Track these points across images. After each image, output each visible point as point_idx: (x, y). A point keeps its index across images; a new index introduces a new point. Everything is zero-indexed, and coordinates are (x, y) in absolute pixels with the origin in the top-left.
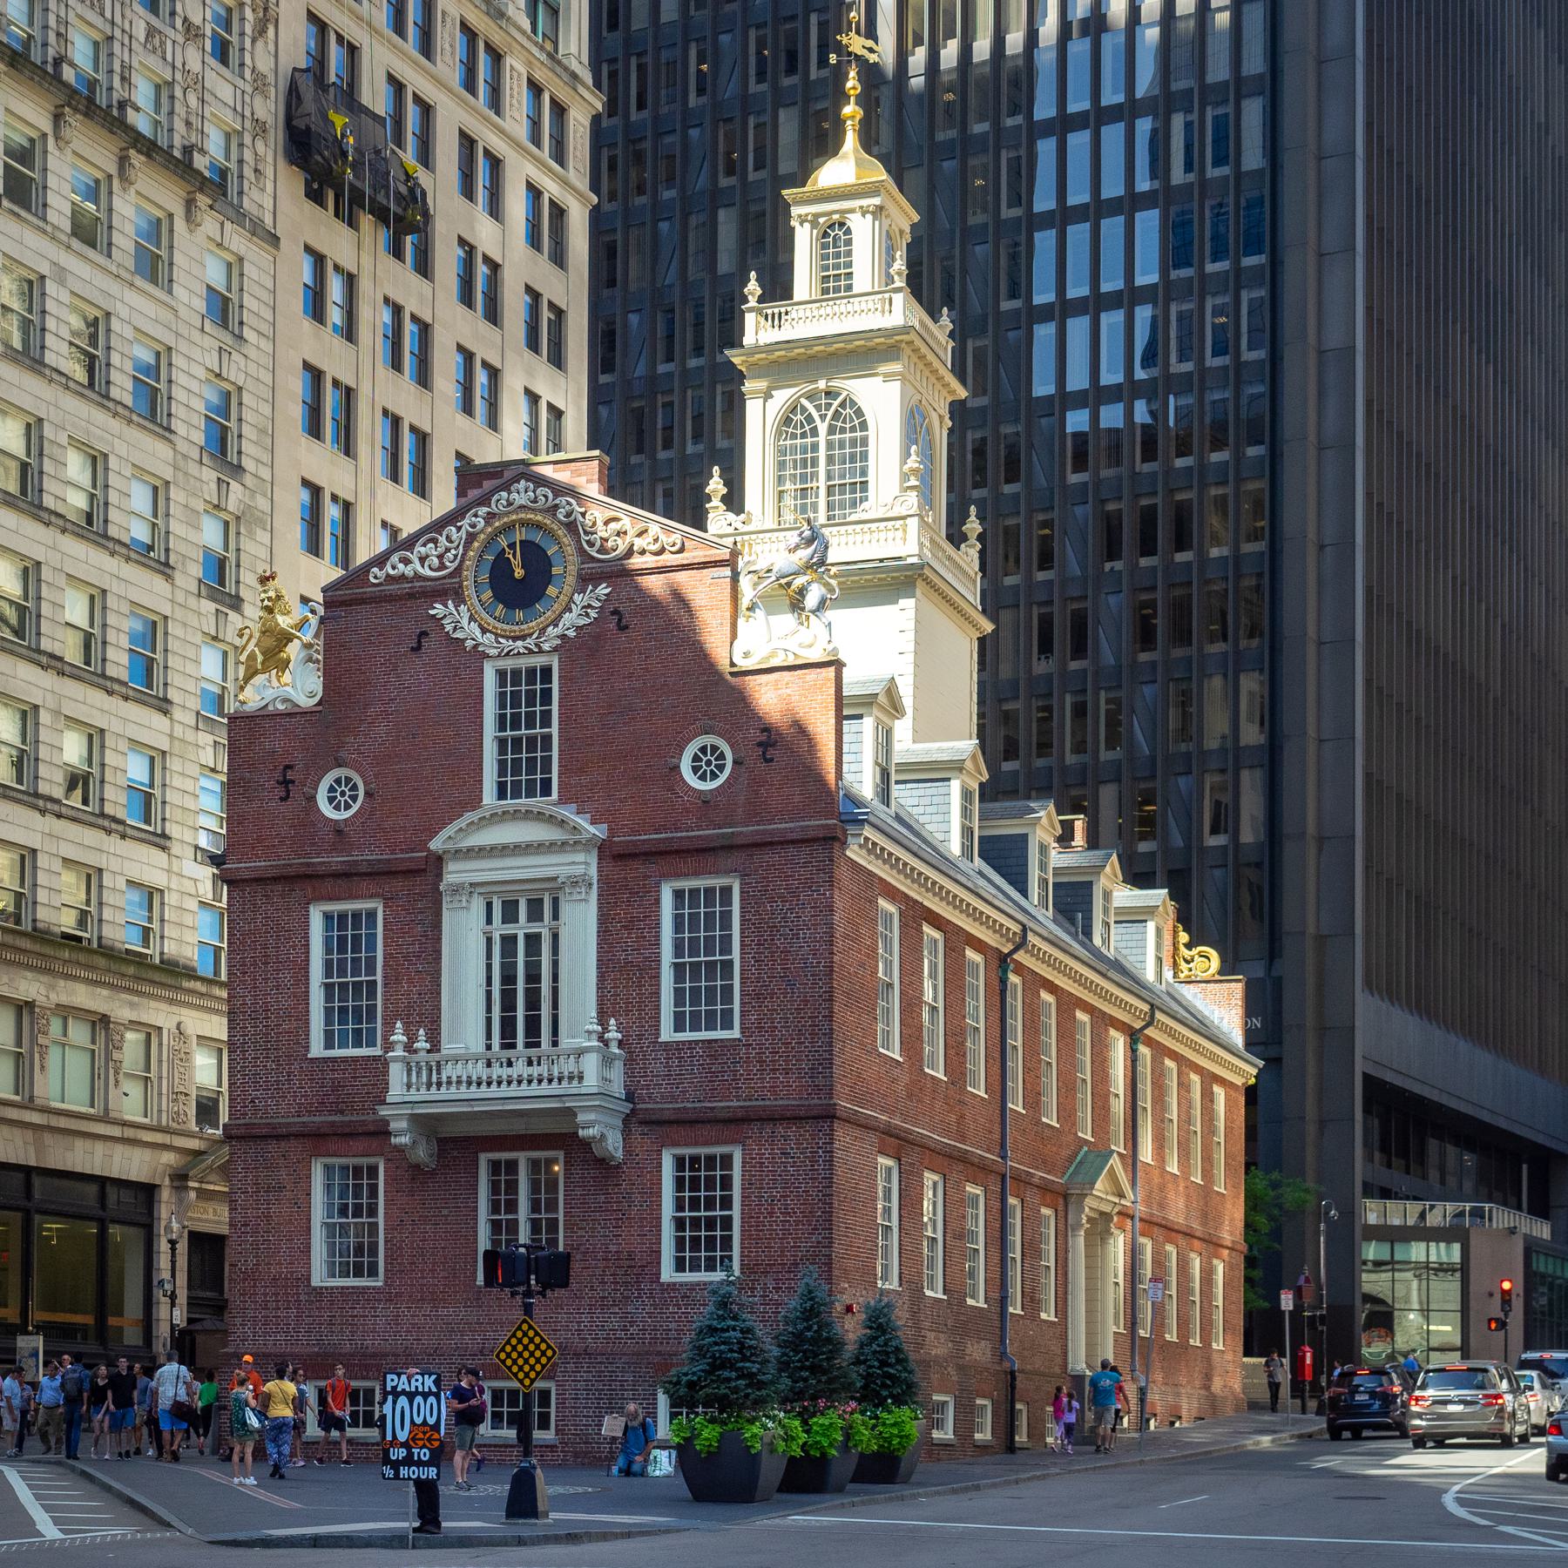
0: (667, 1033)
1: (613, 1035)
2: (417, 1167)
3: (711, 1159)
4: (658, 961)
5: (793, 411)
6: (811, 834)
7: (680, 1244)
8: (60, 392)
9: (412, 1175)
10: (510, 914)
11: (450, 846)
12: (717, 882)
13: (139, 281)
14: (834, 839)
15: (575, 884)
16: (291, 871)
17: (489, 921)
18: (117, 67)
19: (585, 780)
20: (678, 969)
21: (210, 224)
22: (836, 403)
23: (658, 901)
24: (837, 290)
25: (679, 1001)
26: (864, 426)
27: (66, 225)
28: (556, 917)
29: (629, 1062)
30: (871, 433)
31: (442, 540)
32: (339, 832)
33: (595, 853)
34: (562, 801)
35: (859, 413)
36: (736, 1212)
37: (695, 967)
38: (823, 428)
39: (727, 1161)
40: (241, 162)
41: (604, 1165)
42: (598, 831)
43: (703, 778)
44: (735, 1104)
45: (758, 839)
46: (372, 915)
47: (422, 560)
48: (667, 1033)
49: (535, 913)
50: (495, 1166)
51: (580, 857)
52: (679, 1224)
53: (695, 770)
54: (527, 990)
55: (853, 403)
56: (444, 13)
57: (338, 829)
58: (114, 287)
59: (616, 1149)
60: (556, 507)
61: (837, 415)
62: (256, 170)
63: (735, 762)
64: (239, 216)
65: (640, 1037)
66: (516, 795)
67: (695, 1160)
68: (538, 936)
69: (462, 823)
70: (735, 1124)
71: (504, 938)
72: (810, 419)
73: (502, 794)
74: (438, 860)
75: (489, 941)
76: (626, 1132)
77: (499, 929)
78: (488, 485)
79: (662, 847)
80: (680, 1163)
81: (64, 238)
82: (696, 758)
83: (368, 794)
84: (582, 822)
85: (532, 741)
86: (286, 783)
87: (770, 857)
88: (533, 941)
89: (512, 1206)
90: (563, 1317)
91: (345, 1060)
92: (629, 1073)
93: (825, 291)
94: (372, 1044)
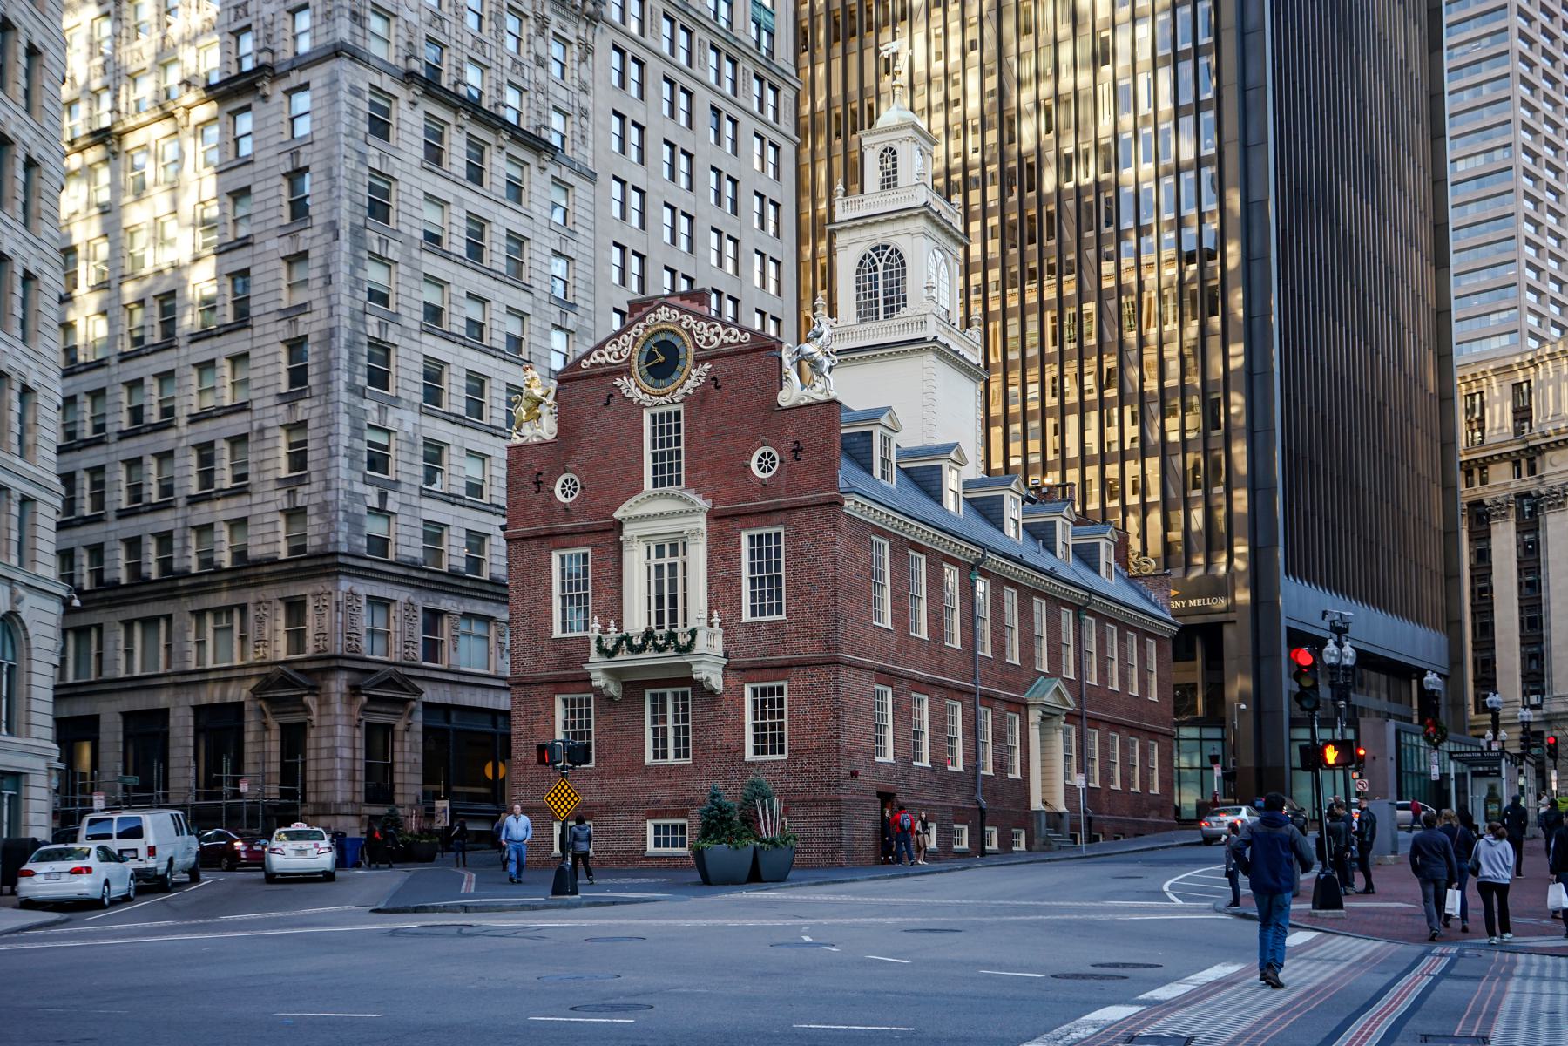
0: (746, 617)
1: (716, 620)
2: (611, 699)
3: (772, 689)
4: (740, 577)
5: (864, 258)
6: (822, 501)
8: (461, 268)
10: (660, 554)
11: (626, 515)
12: (772, 530)
13: (509, 204)
14: (836, 503)
16: (541, 533)
18: (494, 84)
19: (699, 474)
20: (753, 580)
21: (553, 170)
22: (887, 252)
23: (739, 542)
24: (889, 187)
26: (903, 264)
27: (464, 174)
29: (725, 635)
30: (907, 267)
31: (620, 342)
32: (567, 510)
34: (686, 488)
35: (901, 257)
36: (786, 720)
37: (762, 579)
38: (880, 266)
39: (780, 689)
40: (572, 132)
41: (712, 692)
42: (706, 505)
43: (763, 471)
45: (794, 505)
47: (610, 354)
49: (674, 553)
50: (654, 697)
52: (756, 727)
53: (760, 466)
54: (670, 596)
55: (897, 251)
56: (699, 40)
57: (566, 509)
58: (494, 207)
60: (681, 320)
61: (888, 259)
62: (582, 137)
63: (781, 461)
64: (571, 165)
65: (731, 620)
66: (663, 485)
67: (763, 690)
68: (675, 564)
69: (631, 501)
70: (784, 668)
71: (657, 566)
72: (873, 262)
73: (655, 486)
74: (619, 525)
76: (725, 676)
78: (645, 309)
79: (741, 512)
80: (755, 691)
81: (462, 182)
82: (760, 460)
83: (582, 488)
84: (698, 500)
85: (670, 453)
86: (538, 483)
87: (801, 515)
88: (673, 566)
89: (664, 719)
90: (691, 783)
91: (571, 639)
92: (725, 642)
93: (883, 188)
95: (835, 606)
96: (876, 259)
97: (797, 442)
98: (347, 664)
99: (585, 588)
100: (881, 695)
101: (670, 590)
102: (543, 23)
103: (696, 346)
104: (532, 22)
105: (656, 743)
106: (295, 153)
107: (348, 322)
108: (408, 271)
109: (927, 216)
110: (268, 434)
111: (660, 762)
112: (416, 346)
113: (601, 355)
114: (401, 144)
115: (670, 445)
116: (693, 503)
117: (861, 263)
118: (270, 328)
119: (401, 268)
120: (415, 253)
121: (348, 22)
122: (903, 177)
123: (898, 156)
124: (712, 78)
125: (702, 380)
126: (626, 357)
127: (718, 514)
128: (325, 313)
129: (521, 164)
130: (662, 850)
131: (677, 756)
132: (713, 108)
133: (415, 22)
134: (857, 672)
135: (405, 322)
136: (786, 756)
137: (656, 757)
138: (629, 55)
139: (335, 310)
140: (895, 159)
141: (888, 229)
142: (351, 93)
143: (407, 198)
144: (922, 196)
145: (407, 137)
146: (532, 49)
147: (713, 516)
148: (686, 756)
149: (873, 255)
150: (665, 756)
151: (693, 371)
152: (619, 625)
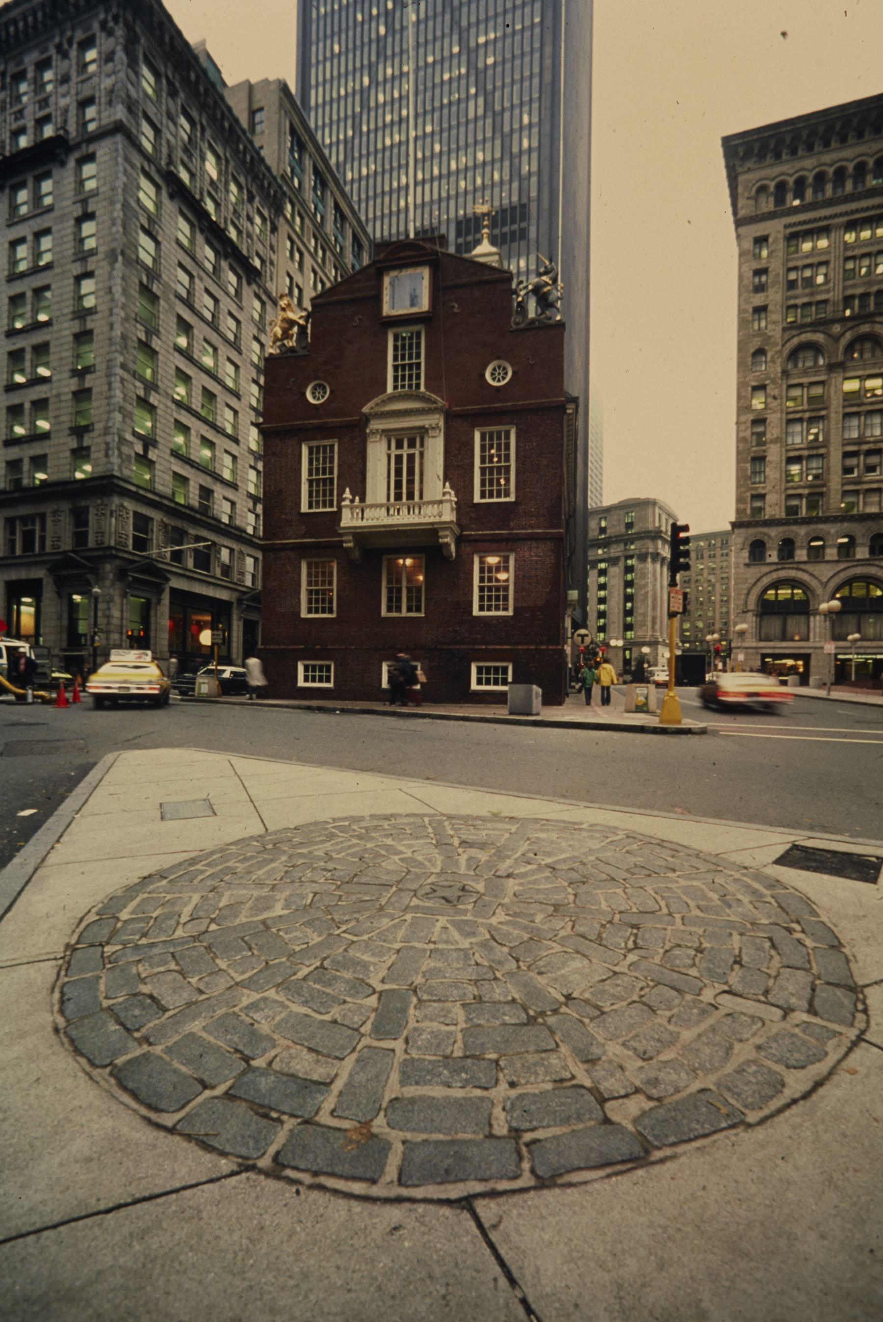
7: (481, 598)
9: (350, 567)
10: (399, 445)
15: (433, 428)
17: (389, 448)
20: (483, 470)
23: (473, 438)
25: (483, 483)
28: (422, 445)
43: (494, 379)
46: (332, 447)
48: (477, 499)
49: (412, 445)
51: (437, 416)
52: (481, 589)
53: (492, 374)
74: (367, 419)
75: (389, 457)
77: (394, 452)
88: (411, 458)
94: (331, 506)
99: (331, 472)
101: (408, 475)
102: (251, 199)
105: (390, 599)
106: (84, 202)
108: (166, 306)
110: (63, 398)
111: (394, 614)
112: (171, 358)
115: (410, 358)
116: (435, 402)
118: (66, 325)
119: (162, 302)
120: (172, 297)
129: (239, 278)
130: (309, 685)
131: (409, 609)
135: (164, 338)
136: (510, 613)
137: (389, 609)
147: (450, 417)
148: (418, 610)
150: (399, 609)
152: (363, 500)
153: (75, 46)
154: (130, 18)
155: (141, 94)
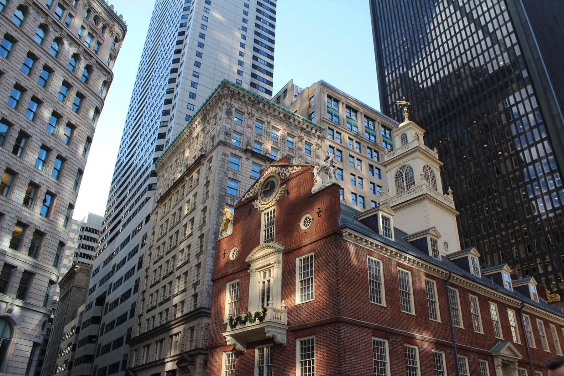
5: (397, 172)
26: (412, 171)
30: (414, 171)
33: (281, 253)
35: (411, 168)
38: (404, 174)
42: (282, 248)
44: (313, 321)
53: (304, 225)
55: (409, 166)
59: (283, 341)
61: (406, 170)
67: (305, 341)
72: (401, 173)
76: (287, 335)
82: (305, 222)
92: (288, 317)
95: (337, 289)
96: (402, 172)
97: (319, 208)
98: (203, 352)
100: (382, 344)
103: (281, 179)
104: (297, 138)
106: (207, 177)
107: (215, 226)
109: (420, 151)
113: (248, 194)
114: (242, 171)
117: (396, 175)
121: (224, 136)
122: (409, 140)
123: (408, 136)
124: (369, 156)
125: (282, 192)
126: (256, 192)
127: (287, 252)
128: (209, 224)
132: (369, 165)
133: (251, 136)
134: (357, 328)
138: (335, 148)
139: (211, 222)
140: (406, 137)
141: (405, 159)
142: (223, 155)
143: (243, 187)
144: (416, 144)
145: (244, 169)
146: (297, 145)
149: (401, 170)
151: (280, 190)
153: (212, 119)
154: (229, 101)
155: (233, 124)
